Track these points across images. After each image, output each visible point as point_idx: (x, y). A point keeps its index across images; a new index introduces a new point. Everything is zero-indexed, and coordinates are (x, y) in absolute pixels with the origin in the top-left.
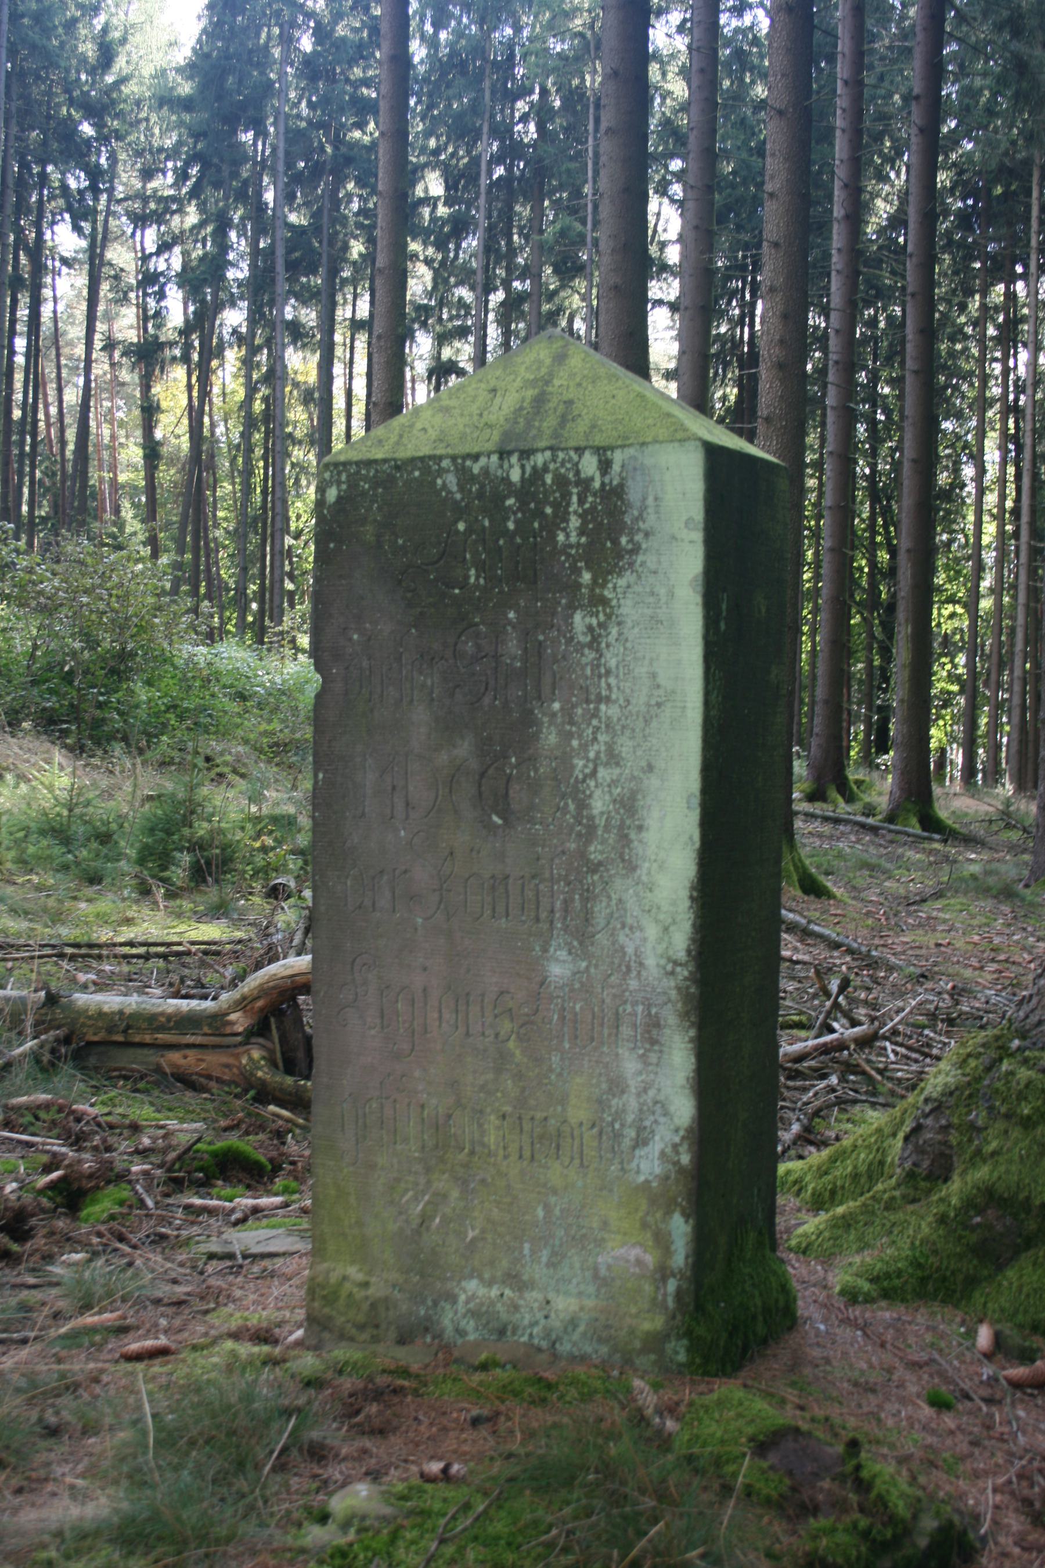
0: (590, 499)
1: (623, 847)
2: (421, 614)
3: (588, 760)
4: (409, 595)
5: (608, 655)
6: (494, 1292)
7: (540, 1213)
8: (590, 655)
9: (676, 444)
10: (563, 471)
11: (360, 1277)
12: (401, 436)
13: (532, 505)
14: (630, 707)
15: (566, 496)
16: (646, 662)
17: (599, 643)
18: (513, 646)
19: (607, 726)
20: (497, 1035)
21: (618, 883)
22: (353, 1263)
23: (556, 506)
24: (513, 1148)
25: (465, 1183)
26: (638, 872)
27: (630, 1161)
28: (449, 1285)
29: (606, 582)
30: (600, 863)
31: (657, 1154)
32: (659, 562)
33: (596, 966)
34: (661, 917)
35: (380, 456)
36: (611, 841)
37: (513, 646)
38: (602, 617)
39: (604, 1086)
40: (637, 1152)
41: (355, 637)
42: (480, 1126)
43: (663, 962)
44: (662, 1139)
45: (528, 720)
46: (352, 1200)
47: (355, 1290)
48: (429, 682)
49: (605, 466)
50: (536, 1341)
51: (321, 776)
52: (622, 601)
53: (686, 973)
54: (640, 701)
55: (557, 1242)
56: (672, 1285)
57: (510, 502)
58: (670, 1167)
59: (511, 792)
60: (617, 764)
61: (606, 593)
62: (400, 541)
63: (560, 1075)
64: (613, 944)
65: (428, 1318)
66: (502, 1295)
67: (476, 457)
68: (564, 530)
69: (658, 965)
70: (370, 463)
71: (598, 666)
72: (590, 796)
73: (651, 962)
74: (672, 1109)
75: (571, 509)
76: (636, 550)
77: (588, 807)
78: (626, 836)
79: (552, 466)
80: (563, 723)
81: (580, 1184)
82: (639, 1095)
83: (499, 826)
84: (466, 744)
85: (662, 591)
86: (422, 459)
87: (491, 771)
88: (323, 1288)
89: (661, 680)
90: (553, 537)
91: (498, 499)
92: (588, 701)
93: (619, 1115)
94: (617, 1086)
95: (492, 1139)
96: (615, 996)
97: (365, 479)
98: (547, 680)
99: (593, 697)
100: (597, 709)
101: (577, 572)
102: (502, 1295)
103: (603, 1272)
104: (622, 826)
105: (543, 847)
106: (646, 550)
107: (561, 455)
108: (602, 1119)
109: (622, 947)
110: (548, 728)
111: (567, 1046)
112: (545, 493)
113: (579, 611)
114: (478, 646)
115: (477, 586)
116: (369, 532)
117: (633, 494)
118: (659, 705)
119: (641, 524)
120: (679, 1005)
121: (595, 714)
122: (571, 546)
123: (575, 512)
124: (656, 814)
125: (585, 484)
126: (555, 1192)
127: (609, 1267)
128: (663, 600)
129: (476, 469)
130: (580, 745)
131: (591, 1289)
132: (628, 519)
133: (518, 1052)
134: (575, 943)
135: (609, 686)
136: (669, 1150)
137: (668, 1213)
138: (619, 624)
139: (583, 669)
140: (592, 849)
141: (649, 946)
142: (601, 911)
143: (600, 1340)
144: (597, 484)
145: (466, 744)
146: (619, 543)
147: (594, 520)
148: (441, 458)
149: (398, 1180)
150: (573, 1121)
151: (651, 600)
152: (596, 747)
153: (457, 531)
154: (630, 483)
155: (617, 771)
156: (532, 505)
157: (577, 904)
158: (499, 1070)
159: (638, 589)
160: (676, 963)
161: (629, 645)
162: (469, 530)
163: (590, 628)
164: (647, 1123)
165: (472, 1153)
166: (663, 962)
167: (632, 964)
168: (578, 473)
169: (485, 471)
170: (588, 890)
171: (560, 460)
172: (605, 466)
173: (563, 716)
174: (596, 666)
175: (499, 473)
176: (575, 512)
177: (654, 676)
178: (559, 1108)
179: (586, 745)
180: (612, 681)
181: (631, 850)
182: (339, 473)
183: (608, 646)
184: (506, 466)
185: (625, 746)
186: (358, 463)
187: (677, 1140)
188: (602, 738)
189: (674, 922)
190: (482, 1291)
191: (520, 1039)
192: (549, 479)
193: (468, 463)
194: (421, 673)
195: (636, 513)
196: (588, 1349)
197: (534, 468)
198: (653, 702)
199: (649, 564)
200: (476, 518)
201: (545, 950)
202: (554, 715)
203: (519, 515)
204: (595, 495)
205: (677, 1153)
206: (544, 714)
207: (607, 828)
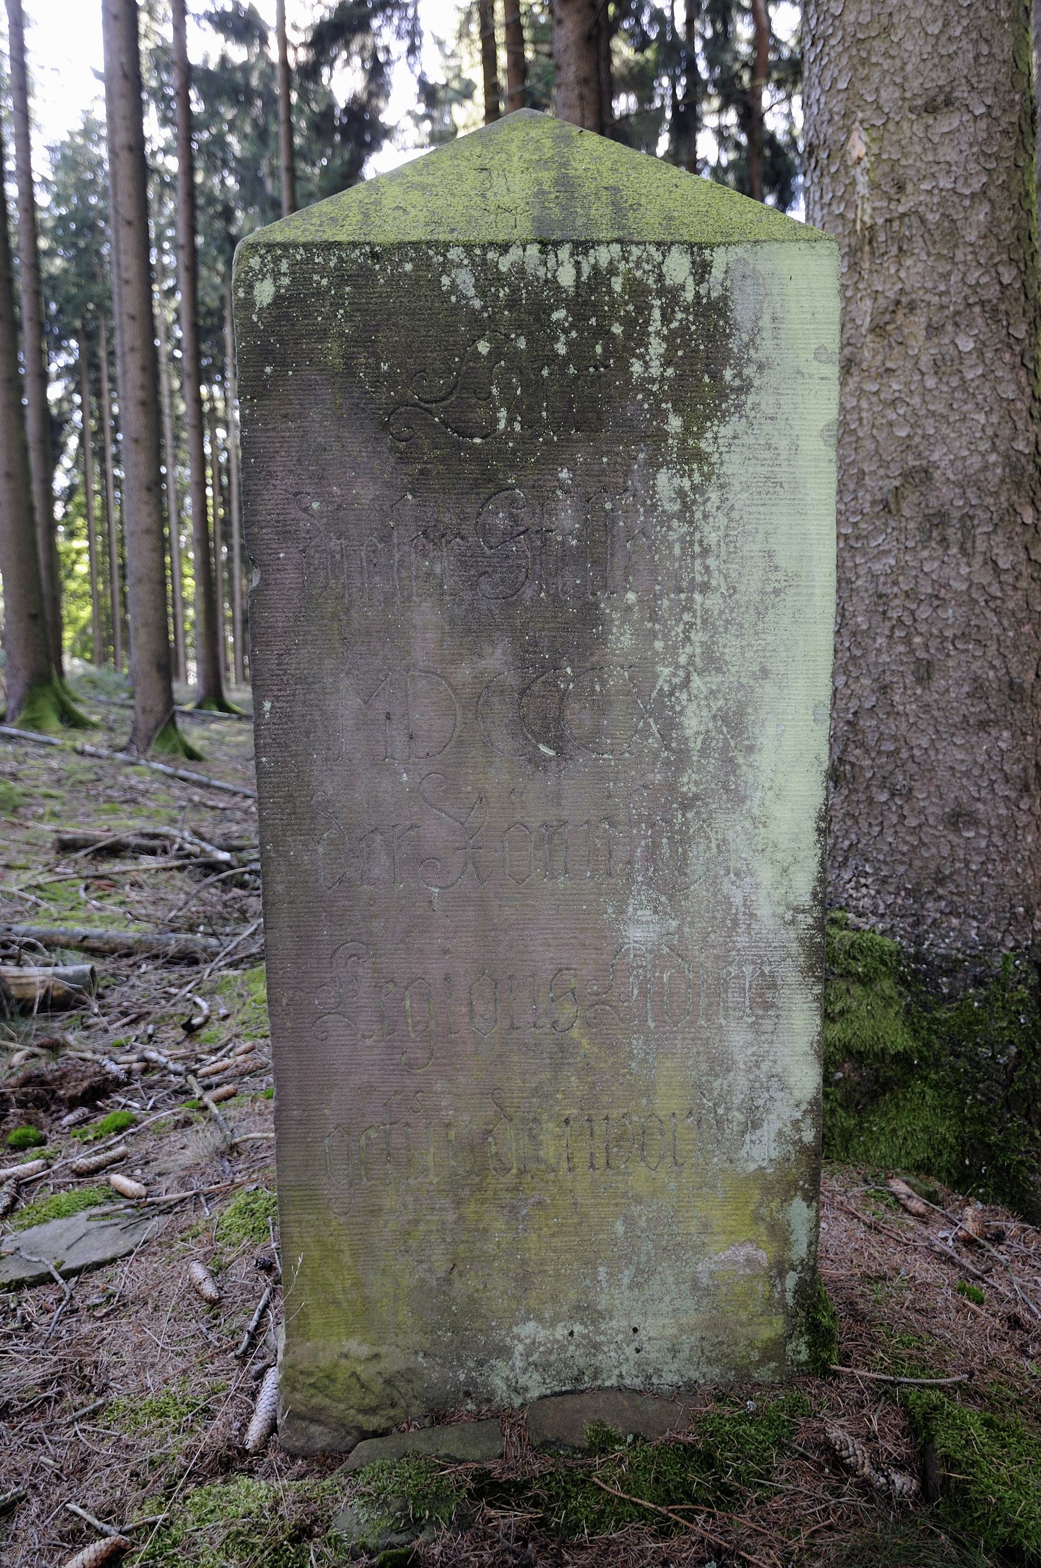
0: (679, 316)
1: (727, 774)
2: (422, 472)
3: (678, 667)
4: (402, 445)
5: (707, 529)
6: (560, 1332)
7: (620, 1228)
8: (679, 528)
9: (802, 245)
10: (638, 274)
11: (365, 1350)
12: (366, 215)
13: (593, 321)
14: (737, 596)
15: (643, 309)
16: (760, 537)
17: (692, 512)
19: (704, 622)
20: (554, 1024)
21: (720, 818)
22: (350, 1334)
23: (629, 323)
24: (581, 1159)
25: (513, 1209)
26: (749, 803)
27: (737, 1150)
28: (497, 1336)
29: (703, 430)
30: (696, 797)
31: (773, 1136)
32: (779, 405)
33: (692, 924)
34: (779, 856)
35: (342, 237)
36: (711, 768)
38: (697, 478)
39: (704, 1067)
40: (748, 1137)
41: (315, 505)
42: (533, 1137)
43: (781, 910)
44: (779, 1117)
46: (347, 1258)
47: (359, 1369)
48: (438, 570)
49: (701, 270)
50: (627, 1381)
51: (267, 705)
52: (725, 457)
53: (810, 921)
54: (750, 587)
55: (643, 1258)
56: (791, 1280)
57: (559, 315)
58: (790, 1147)
59: (568, 714)
60: (719, 670)
61: (703, 445)
62: (385, 367)
63: (645, 1060)
64: (715, 895)
65: (471, 1381)
66: (571, 1334)
67: (504, 248)
68: (641, 357)
69: (774, 915)
70: (329, 246)
71: (692, 545)
72: (681, 713)
73: (765, 911)
74: (792, 1081)
75: (651, 329)
76: (745, 388)
77: (679, 726)
78: (731, 760)
79: (622, 266)
80: (642, 620)
81: (673, 1185)
82: (749, 1071)
83: (551, 759)
84: (499, 652)
85: (783, 444)
86: (415, 245)
87: (536, 688)
88: (310, 1374)
89: (781, 561)
90: (625, 368)
91: (541, 311)
92: (681, 591)
93: (723, 1098)
94: (721, 1064)
95: (550, 1151)
96: (717, 957)
97: (323, 271)
98: (619, 561)
99: (684, 584)
100: (690, 600)
101: (662, 416)
102: (571, 1334)
103: (705, 1281)
104: (726, 746)
105: (616, 781)
106: (760, 388)
107: (636, 251)
108: (702, 1106)
109: (727, 898)
110: (619, 627)
111: (652, 1024)
112: (612, 304)
113: (664, 470)
114: (514, 518)
115: (509, 434)
116: (333, 352)
117: (741, 311)
118: (777, 592)
119: (752, 352)
120: (801, 959)
121: (688, 607)
122: (652, 381)
123: (658, 333)
124: (771, 730)
125: (671, 295)
126: (638, 1200)
127: (712, 1274)
128: (784, 455)
129: (504, 264)
130: (666, 647)
131: (689, 1303)
132: (733, 345)
133: (584, 1041)
134: (663, 899)
135: (707, 568)
136: (788, 1130)
137: (787, 1200)
138: (721, 487)
139: (670, 548)
140: (685, 779)
141: (763, 892)
142: (698, 856)
143: (710, 1362)
144: (689, 296)
145: (499, 652)
146: (722, 378)
147: (685, 345)
148: (447, 245)
149: (416, 1222)
150: (661, 1114)
151: (767, 455)
152: (688, 649)
153: (477, 355)
154: (736, 295)
155: (719, 678)
156: (593, 321)
157: (665, 850)
158: (557, 1067)
159: (746, 440)
160: (797, 910)
161: (735, 515)
162: (496, 354)
163: (681, 493)
164: (760, 1102)
165: (522, 1172)
166: (781, 910)
167: (740, 916)
168: (661, 278)
169: (520, 270)
170: (680, 832)
171: (633, 258)
172: (701, 270)
173: (641, 611)
174: (687, 543)
175: (541, 272)
176: (658, 333)
177: (770, 554)
178: (644, 1101)
179: (675, 647)
180: (711, 562)
181: (738, 777)
182: (276, 260)
183: (705, 517)
184: (551, 262)
185: (729, 646)
186: (306, 246)
187: (798, 1115)
188: (696, 637)
189: (796, 861)
190: (542, 1334)
192: (617, 284)
193: (491, 255)
194: (425, 556)
195: (745, 337)
196: (695, 1375)
197: (595, 267)
198: (769, 589)
199: (763, 407)
200: (507, 336)
202: (629, 609)
203: (574, 334)
204: (686, 310)
205: (799, 1130)
206: (614, 609)
207: (703, 752)
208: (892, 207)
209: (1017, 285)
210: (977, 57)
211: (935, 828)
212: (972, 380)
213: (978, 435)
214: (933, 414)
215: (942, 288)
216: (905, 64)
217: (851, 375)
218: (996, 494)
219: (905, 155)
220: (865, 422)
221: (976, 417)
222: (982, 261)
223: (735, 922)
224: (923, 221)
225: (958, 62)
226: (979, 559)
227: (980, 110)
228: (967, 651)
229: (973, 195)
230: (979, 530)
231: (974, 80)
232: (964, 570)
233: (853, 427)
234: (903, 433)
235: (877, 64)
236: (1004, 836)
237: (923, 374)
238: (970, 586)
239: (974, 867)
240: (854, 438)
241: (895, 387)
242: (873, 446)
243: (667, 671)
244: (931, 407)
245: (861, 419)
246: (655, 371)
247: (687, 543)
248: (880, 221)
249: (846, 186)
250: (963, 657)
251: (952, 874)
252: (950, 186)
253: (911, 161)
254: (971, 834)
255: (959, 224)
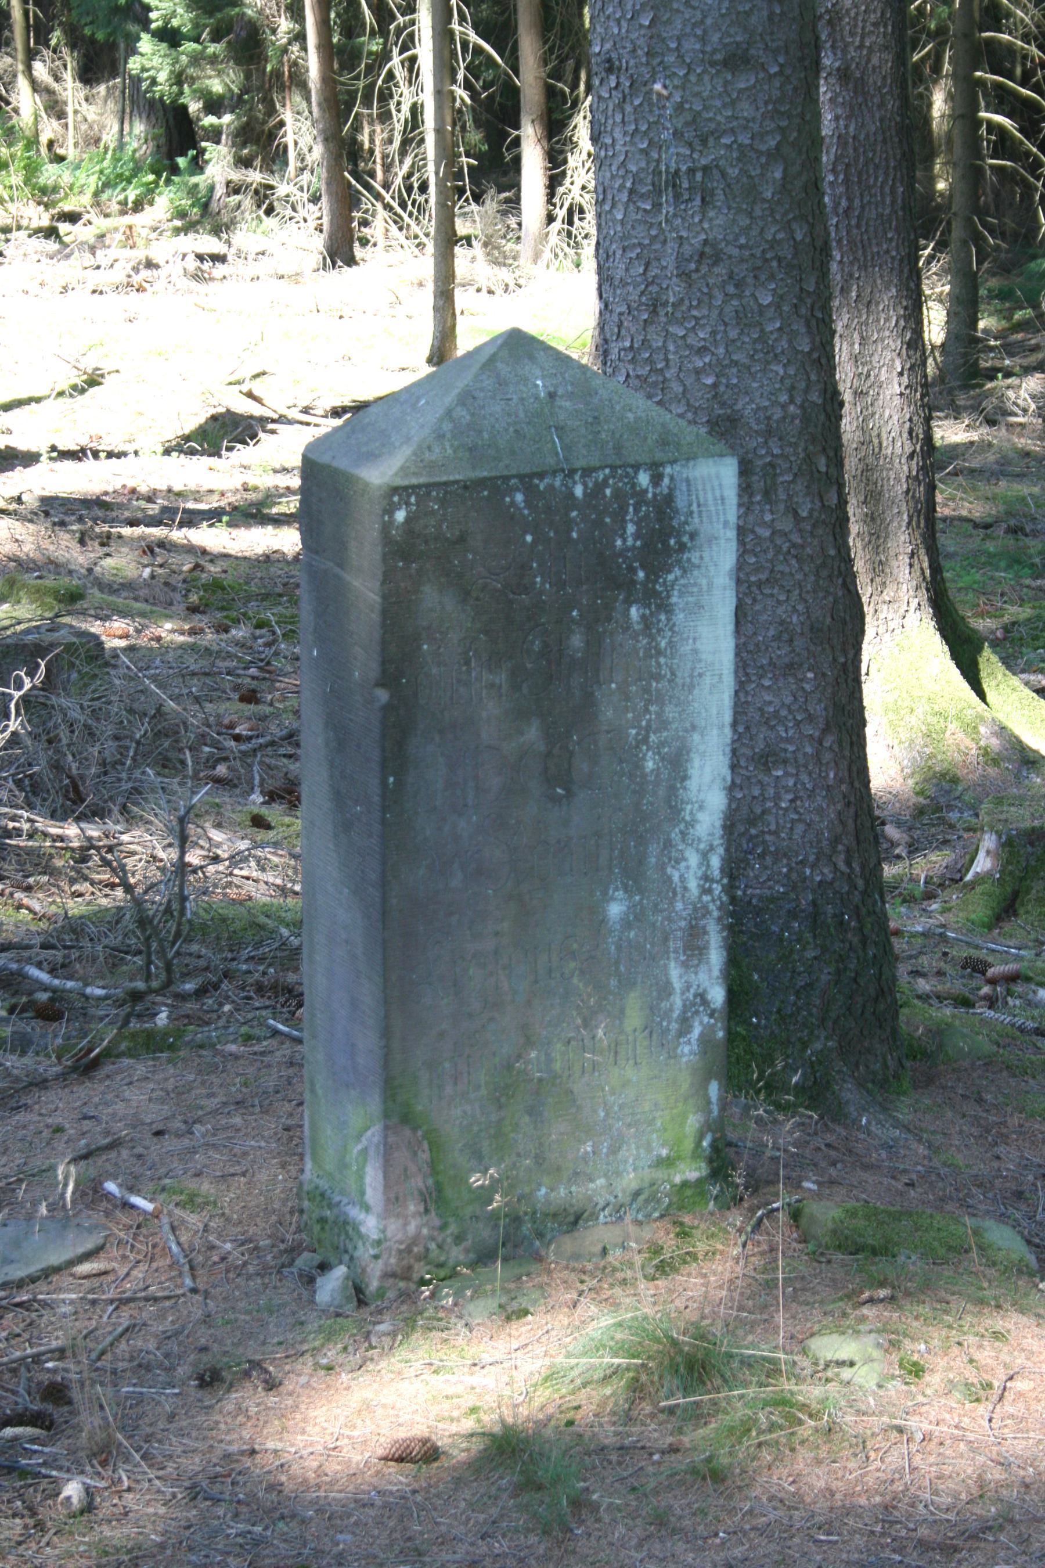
18: (577, 641)
32: (701, 558)
37: (577, 641)
45: (589, 699)
49: (656, 479)
76: (682, 547)
82: (683, 993)
85: (704, 582)
117: (680, 502)
123: (631, 521)
128: (705, 588)
132: (675, 523)
141: (692, 872)
159: (682, 581)
168: (634, 486)
169: (551, 487)
176: (631, 521)
181: (677, 797)
182: (409, 496)
188: (653, 708)
191: (582, 972)
192: (608, 492)
197: (596, 483)
201: (605, 893)
208: (695, 156)
209: (807, 240)
210: (770, 18)
211: (747, 768)
212: (771, 332)
213: (777, 386)
214: (736, 363)
215: (743, 241)
216: (705, 17)
217: (658, 315)
218: (795, 445)
219: (706, 108)
220: (672, 363)
221: (775, 368)
222: (778, 217)
223: (675, 893)
224: (724, 175)
225: (753, 20)
226: (782, 507)
227: (775, 69)
228: (772, 595)
229: (769, 154)
230: (781, 479)
231: (768, 38)
232: (768, 517)
233: (659, 366)
234: (709, 381)
235: (678, 11)
236: (810, 774)
237: (726, 324)
238: (773, 533)
239: (783, 805)
240: (661, 378)
241: (702, 335)
242: (681, 389)
243: (634, 732)
244: (735, 357)
245: (667, 360)
246: (630, 542)
247: (648, 650)
248: (684, 168)
249: (649, 123)
250: (770, 602)
251: (764, 812)
252: (748, 142)
253: (711, 115)
254: (780, 773)
255: (756, 180)
